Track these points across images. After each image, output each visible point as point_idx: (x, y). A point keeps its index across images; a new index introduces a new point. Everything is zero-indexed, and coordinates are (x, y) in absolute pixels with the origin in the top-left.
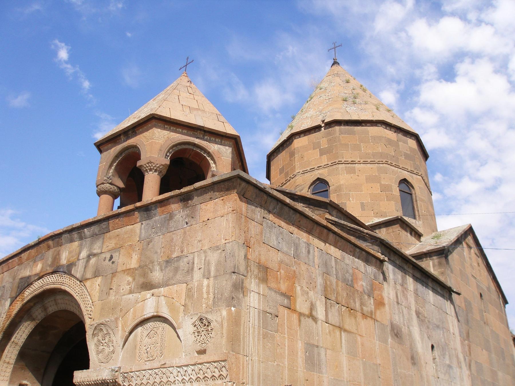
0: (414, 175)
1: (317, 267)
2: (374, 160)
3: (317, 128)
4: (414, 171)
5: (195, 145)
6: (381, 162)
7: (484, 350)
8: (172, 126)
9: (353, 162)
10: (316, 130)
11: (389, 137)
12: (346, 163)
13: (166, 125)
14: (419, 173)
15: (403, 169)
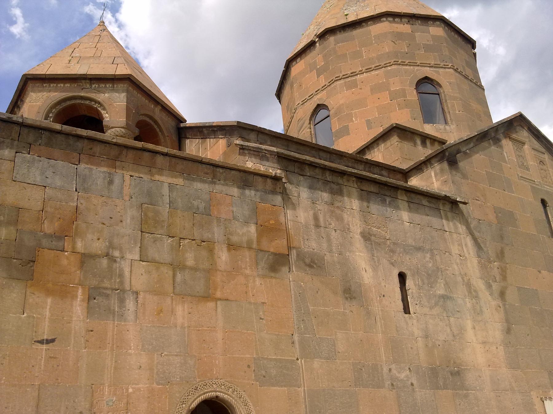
0: (441, 70)
1: (127, 198)
2: (379, 64)
3: (311, 45)
4: (439, 65)
5: (82, 98)
6: (388, 65)
7: (543, 272)
8: (52, 83)
9: (354, 74)
10: (311, 48)
11: (399, 30)
12: (346, 77)
13: (45, 84)
14: (448, 65)
15: (422, 65)
